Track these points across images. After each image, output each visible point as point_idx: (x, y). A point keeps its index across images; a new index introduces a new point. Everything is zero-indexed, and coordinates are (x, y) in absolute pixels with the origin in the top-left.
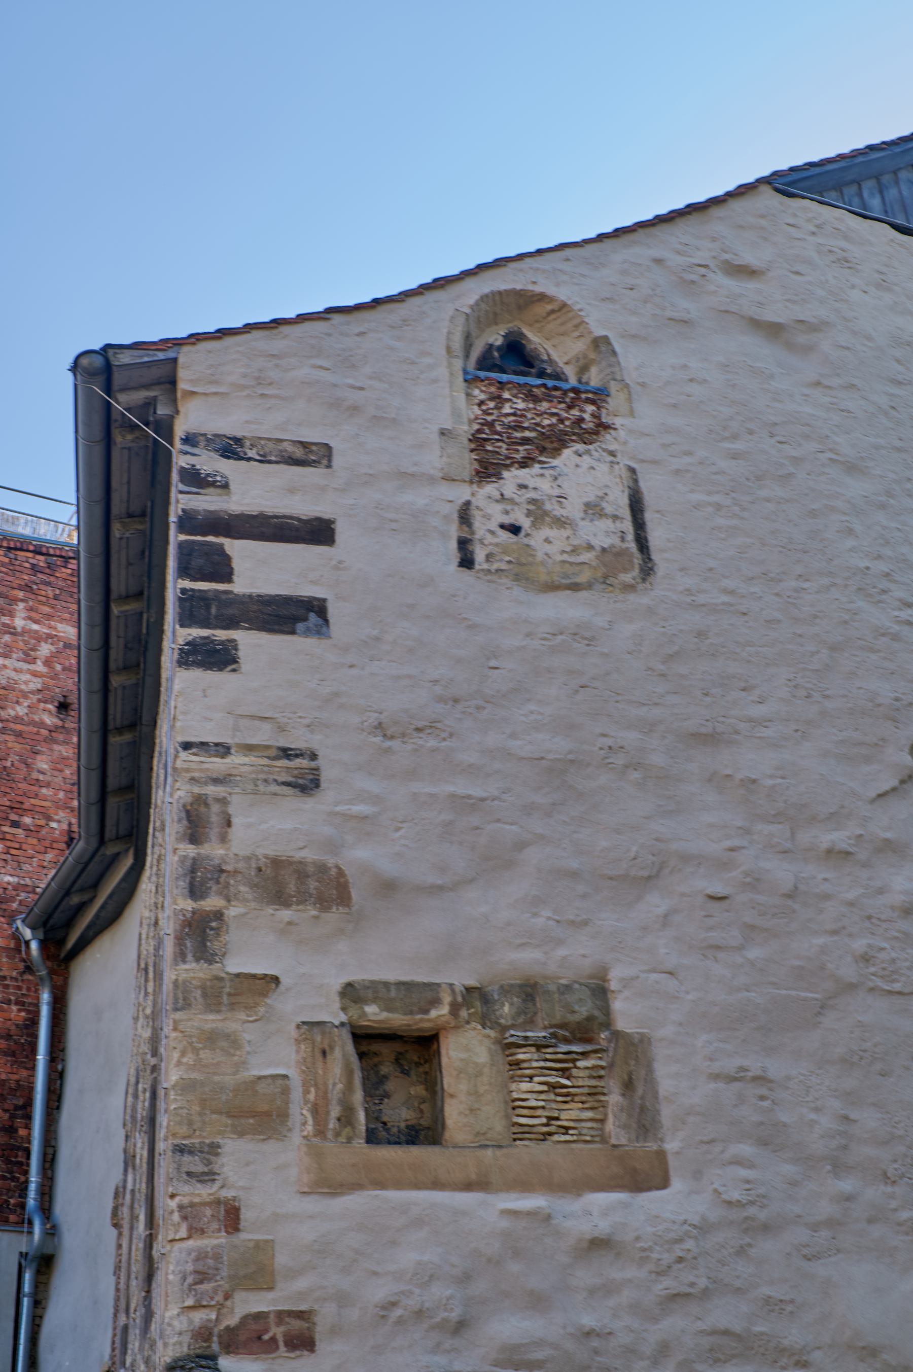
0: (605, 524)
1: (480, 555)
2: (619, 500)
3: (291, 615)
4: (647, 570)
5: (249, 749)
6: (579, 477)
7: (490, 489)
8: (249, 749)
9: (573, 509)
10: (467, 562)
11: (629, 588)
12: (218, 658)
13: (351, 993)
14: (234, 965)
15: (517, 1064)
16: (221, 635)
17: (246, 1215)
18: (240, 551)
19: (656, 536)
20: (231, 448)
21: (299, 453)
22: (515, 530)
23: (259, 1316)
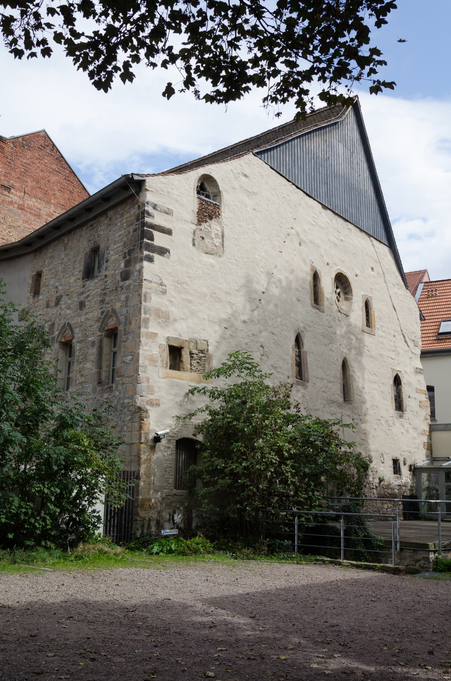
0: (218, 240)
1: (196, 243)
2: (220, 234)
3: (163, 251)
5: (155, 283)
6: (214, 226)
7: (200, 227)
8: (155, 283)
9: (213, 235)
10: (194, 245)
11: (220, 256)
12: (150, 259)
13: (168, 338)
14: (151, 330)
15: (193, 357)
16: (151, 254)
17: (150, 380)
18: (156, 234)
21: (167, 211)
22: (203, 238)
23: (152, 399)
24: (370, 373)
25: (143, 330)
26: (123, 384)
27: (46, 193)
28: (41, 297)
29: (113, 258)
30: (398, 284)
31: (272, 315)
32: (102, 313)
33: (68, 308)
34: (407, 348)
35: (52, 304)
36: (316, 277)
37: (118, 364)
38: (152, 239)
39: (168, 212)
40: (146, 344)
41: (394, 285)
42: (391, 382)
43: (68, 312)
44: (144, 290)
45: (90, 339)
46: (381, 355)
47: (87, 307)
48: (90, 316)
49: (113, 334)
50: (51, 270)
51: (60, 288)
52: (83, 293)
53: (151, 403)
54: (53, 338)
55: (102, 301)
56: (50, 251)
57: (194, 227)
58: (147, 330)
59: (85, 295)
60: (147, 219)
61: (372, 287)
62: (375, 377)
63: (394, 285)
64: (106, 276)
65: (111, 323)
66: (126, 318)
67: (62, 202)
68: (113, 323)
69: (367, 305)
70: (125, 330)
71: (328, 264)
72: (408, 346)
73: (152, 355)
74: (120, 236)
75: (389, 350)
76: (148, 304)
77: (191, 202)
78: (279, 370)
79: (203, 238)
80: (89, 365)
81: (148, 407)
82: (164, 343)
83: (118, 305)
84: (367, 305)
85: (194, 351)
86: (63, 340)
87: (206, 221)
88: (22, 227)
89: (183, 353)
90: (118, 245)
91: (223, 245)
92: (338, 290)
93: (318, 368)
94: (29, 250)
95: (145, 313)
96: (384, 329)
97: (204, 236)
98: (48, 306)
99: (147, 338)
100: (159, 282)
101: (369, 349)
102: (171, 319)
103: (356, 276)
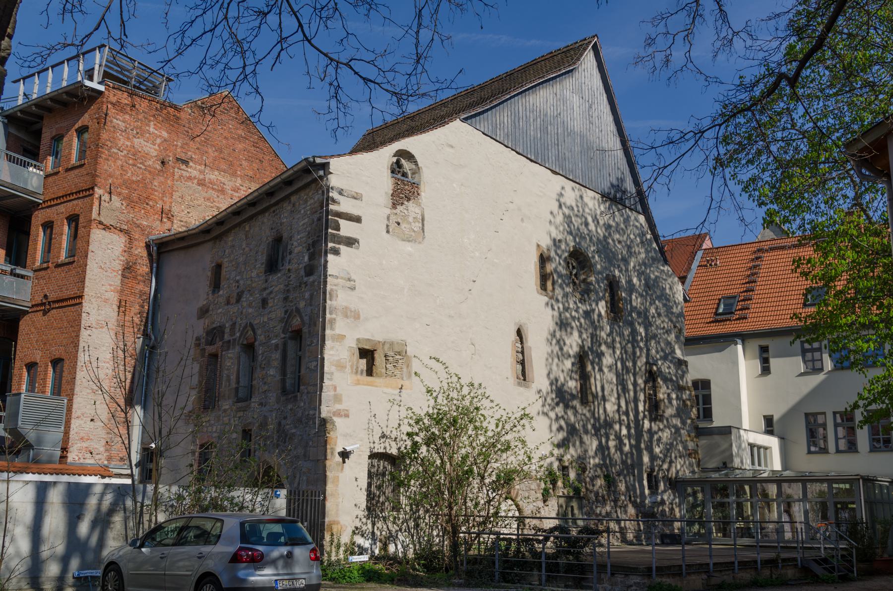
0: (417, 224)
2: (419, 217)
3: (351, 242)
4: (424, 238)
5: (342, 278)
6: (411, 208)
7: (395, 211)
9: (411, 219)
10: (388, 232)
11: (420, 243)
12: (336, 252)
13: (358, 340)
14: (338, 331)
16: (337, 246)
18: (342, 223)
19: (426, 228)
20: (341, 192)
22: (399, 224)
25: (328, 332)
26: (308, 393)
27: (231, 164)
28: (221, 292)
29: (296, 250)
32: (286, 312)
33: (250, 306)
35: (233, 300)
37: (303, 371)
38: (338, 228)
39: (356, 197)
40: (332, 348)
43: (250, 310)
44: (329, 288)
45: (273, 342)
47: (270, 305)
48: (273, 315)
49: (297, 335)
50: (231, 261)
51: (241, 282)
52: (265, 289)
53: (338, 414)
54: (234, 340)
55: (286, 299)
56: (230, 239)
57: (388, 211)
58: (333, 332)
59: (267, 291)
60: (331, 207)
64: (289, 270)
65: (296, 322)
66: (310, 319)
67: (251, 173)
68: (297, 323)
70: (309, 332)
73: (339, 361)
74: (303, 224)
76: (334, 303)
77: (386, 183)
79: (399, 224)
80: (272, 372)
81: (335, 419)
82: (354, 345)
83: (302, 305)
85: (391, 353)
86: (245, 342)
87: (402, 204)
88: (203, 206)
89: (376, 355)
90: (302, 235)
91: (423, 229)
94: (208, 237)
95: (331, 313)
97: (400, 221)
98: (228, 303)
99: (333, 341)
100: (347, 277)
102: (362, 317)
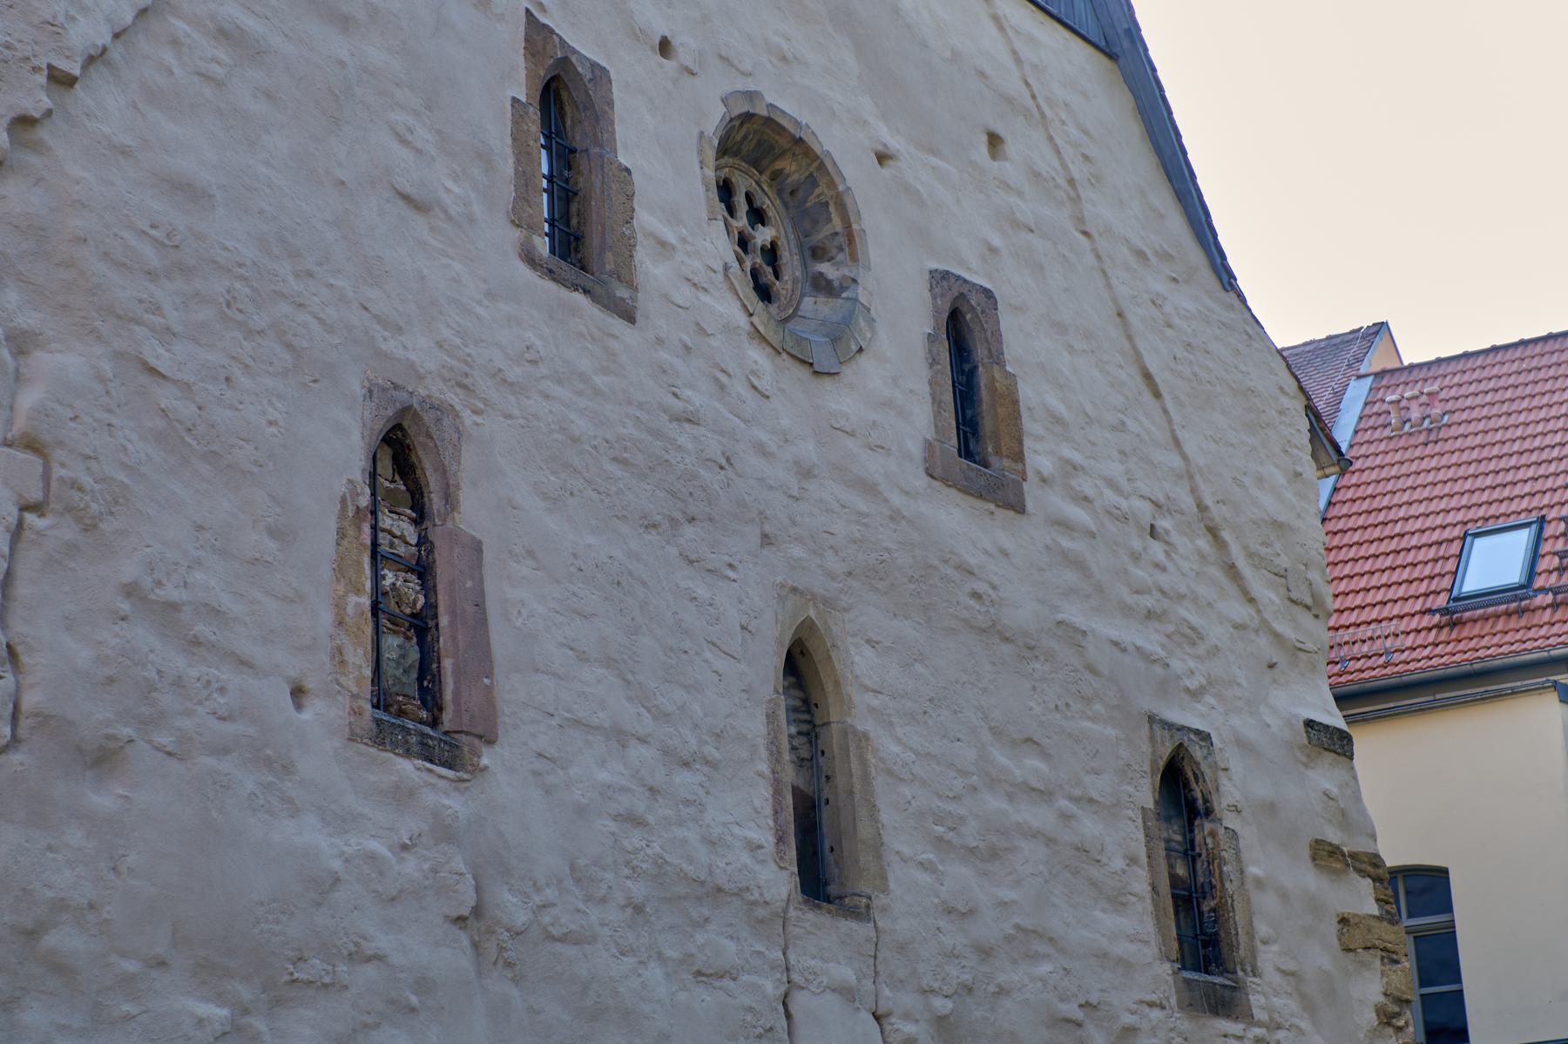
24: (996, 732)
30: (1166, 257)
31: (148, 251)
34: (1240, 611)
36: (562, 103)
41: (1140, 254)
42: (1145, 793)
46: (1074, 635)
61: (997, 241)
62: (1034, 763)
63: (1140, 254)
69: (962, 333)
71: (665, 47)
72: (1252, 600)
75: (1127, 611)
78: (202, 629)
84: (962, 333)
92: (763, 236)
93: (583, 657)
96: (1085, 485)
101: (982, 587)
103: (882, 158)
